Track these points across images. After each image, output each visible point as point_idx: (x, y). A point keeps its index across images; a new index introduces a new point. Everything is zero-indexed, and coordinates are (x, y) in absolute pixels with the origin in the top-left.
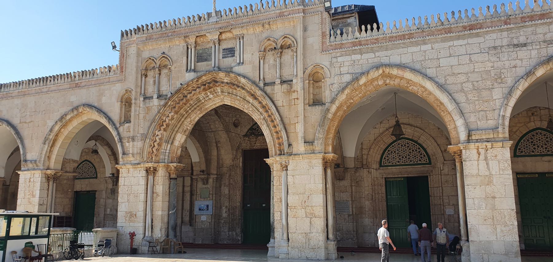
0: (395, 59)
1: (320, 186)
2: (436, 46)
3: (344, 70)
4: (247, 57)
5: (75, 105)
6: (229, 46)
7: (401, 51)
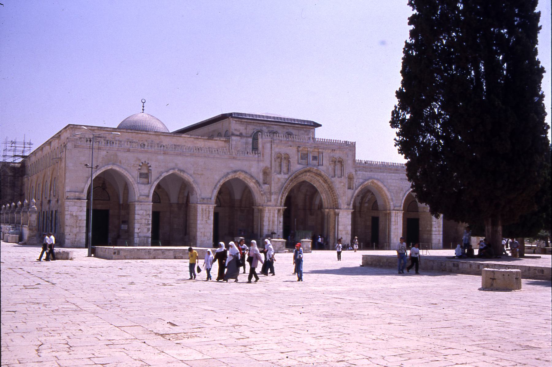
0: (376, 176)
1: (350, 223)
2: (388, 174)
3: (360, 177)
4: (325, 162)
5: (234, 169)
6: (316, 155)
7: (377, 173)
